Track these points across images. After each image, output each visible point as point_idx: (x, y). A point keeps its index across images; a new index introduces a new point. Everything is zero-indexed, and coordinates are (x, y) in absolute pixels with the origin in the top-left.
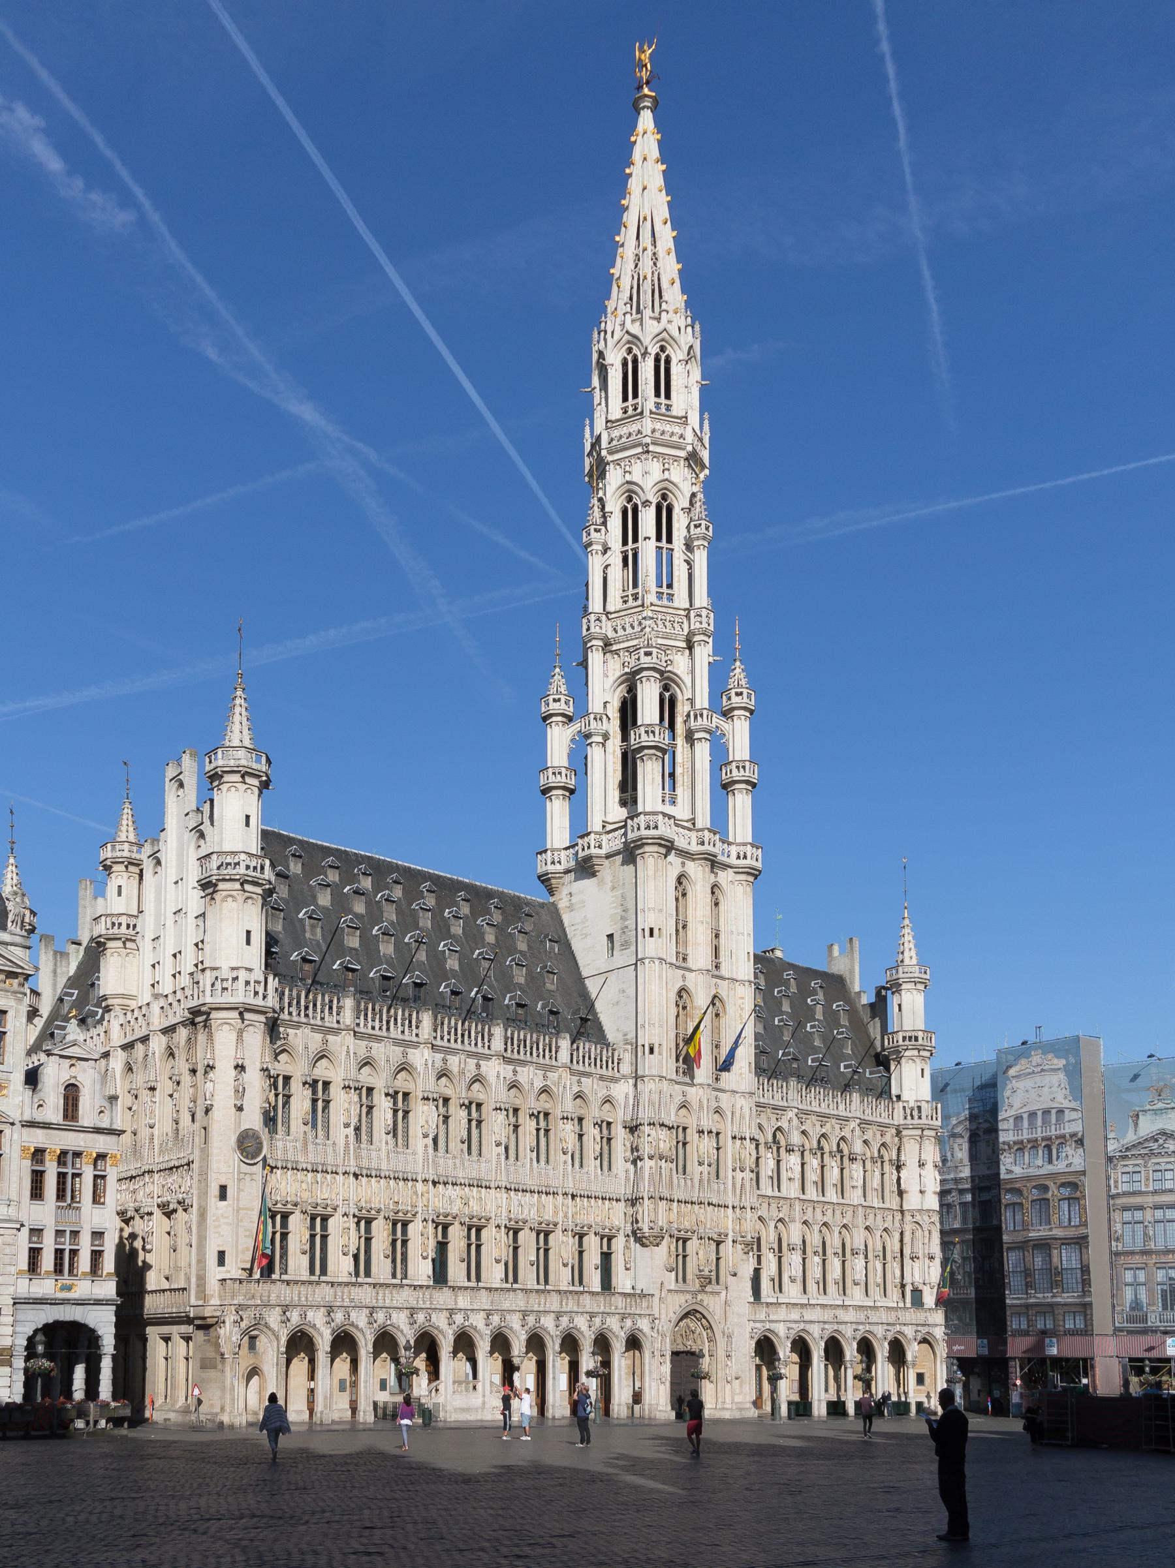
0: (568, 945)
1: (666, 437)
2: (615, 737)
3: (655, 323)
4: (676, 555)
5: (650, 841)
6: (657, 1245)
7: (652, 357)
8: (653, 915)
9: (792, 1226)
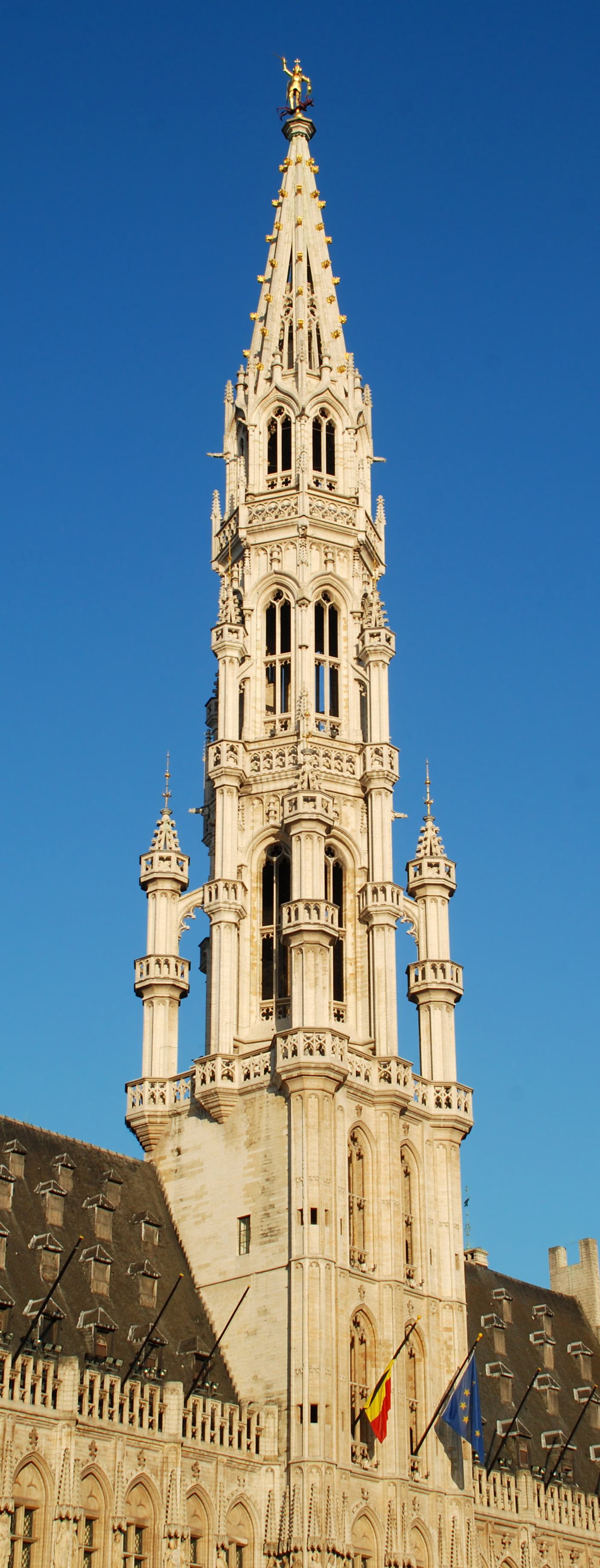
0: (175, 1235)
1: (330, 519)
2: (253, 917)
3: (315, 381)
4: (342, 673)
7: (310, 422)
8: (316, 1188)
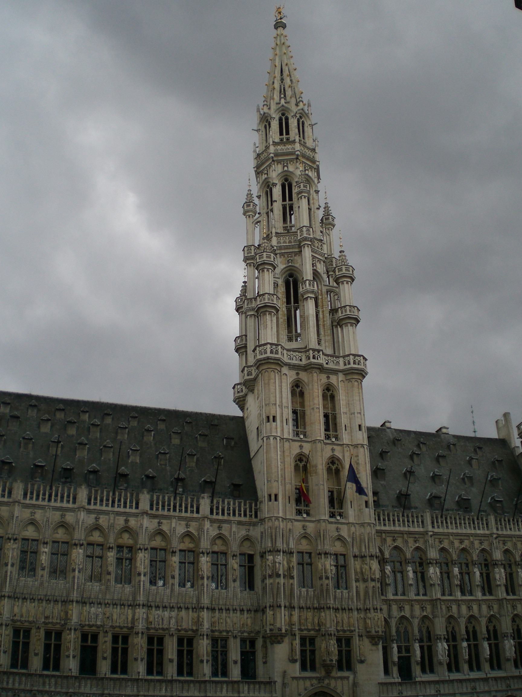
5: (263, 362)
6: (279, 642)
9: (436, 621)
